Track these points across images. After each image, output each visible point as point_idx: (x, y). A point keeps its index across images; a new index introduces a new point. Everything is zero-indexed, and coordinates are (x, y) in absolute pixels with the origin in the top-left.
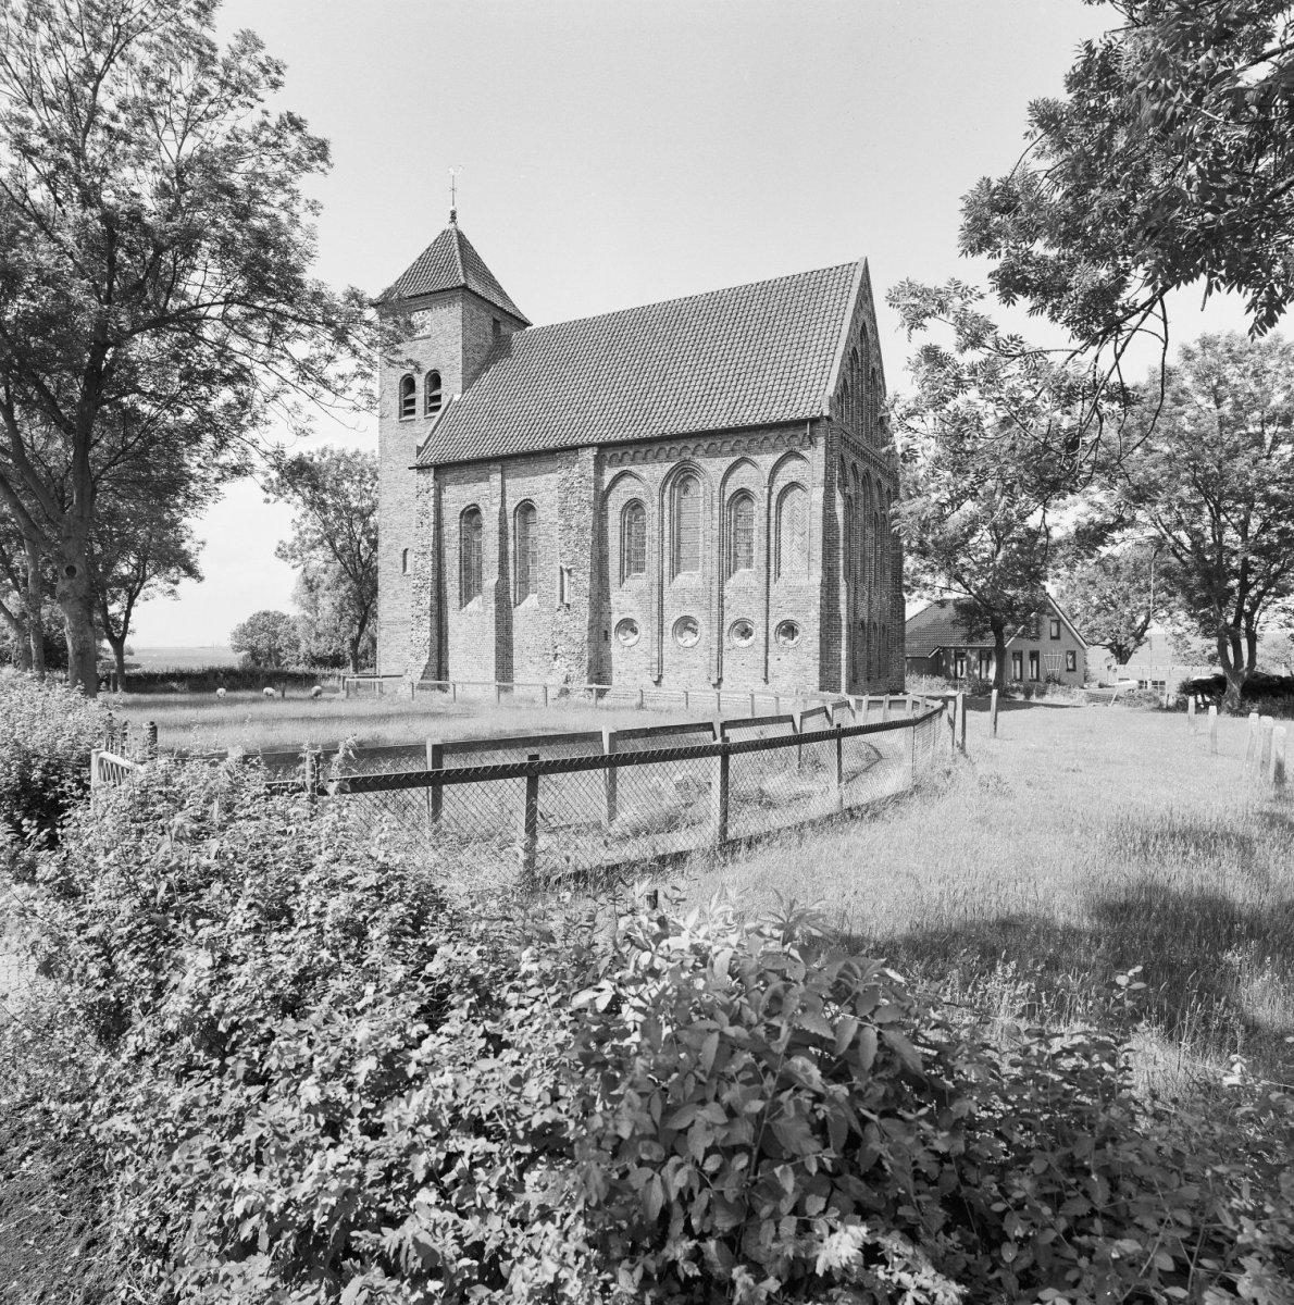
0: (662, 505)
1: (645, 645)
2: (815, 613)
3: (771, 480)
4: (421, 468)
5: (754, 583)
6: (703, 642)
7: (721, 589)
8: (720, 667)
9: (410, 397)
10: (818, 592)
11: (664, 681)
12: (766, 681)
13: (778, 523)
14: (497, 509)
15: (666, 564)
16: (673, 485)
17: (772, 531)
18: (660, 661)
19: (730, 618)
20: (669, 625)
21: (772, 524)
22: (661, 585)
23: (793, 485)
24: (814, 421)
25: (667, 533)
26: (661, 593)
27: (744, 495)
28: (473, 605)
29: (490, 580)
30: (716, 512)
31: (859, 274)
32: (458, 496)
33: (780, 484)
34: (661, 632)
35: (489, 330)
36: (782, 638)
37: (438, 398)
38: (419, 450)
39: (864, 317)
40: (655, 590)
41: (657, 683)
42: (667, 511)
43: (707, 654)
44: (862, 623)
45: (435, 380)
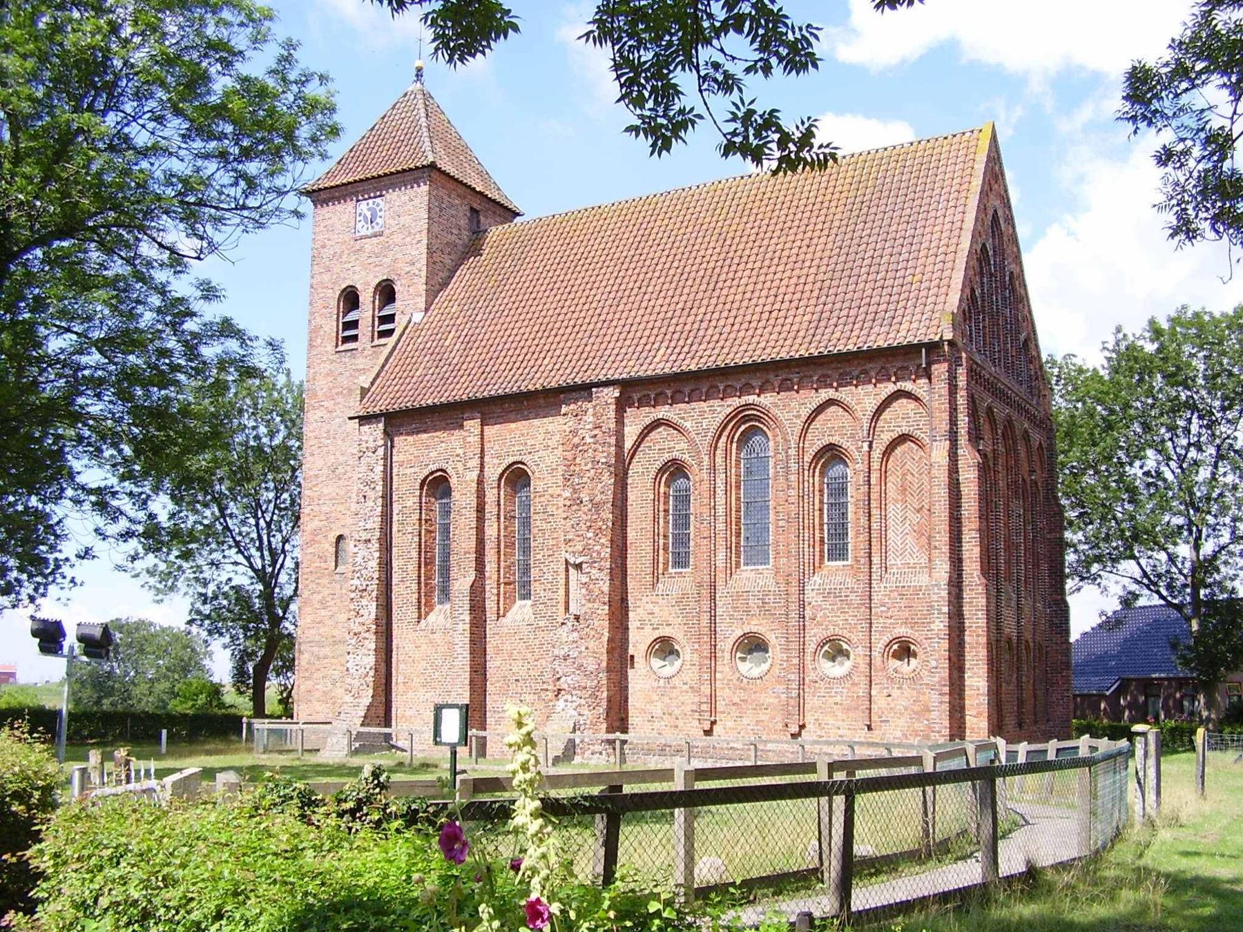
0: (713, 468)
1: (690, 675)
2: (940, 625)
3: (872, 428)
4: (364, 419)
5: (850, 583)
6: (776, 670)
7: (802, 591)
8: (801, 708)
9: (352, 316)
10: (944, 594)
12: (869, 728)
13: (883, 495)
14: (474, 475)
15: (721, 555)
16: (730, 439)
17: (874, 504)
18: (713, 698)
19: (815, 634)
20: (725, 646)
21: (874, 496)
22: (713, 586)
23: (903, 438)
24: (933, 348)
25: (721, 510)
26: (713, 599)
27: (831, 454)
28: (438, 616)
29: (462, 582)
30: (793, 478)
31: (985, 144)
32: (419, 453)
33: (886, 438)
34: (713, 656)
35: (463, 222)
37: (390, 319)
38: (364, 392)
39: (995, 202)
40: (705, 592)
41: (708, 733)
42: (721, 477)
43: (781, 688)
44: (1009, 641)
45: (387, 292)
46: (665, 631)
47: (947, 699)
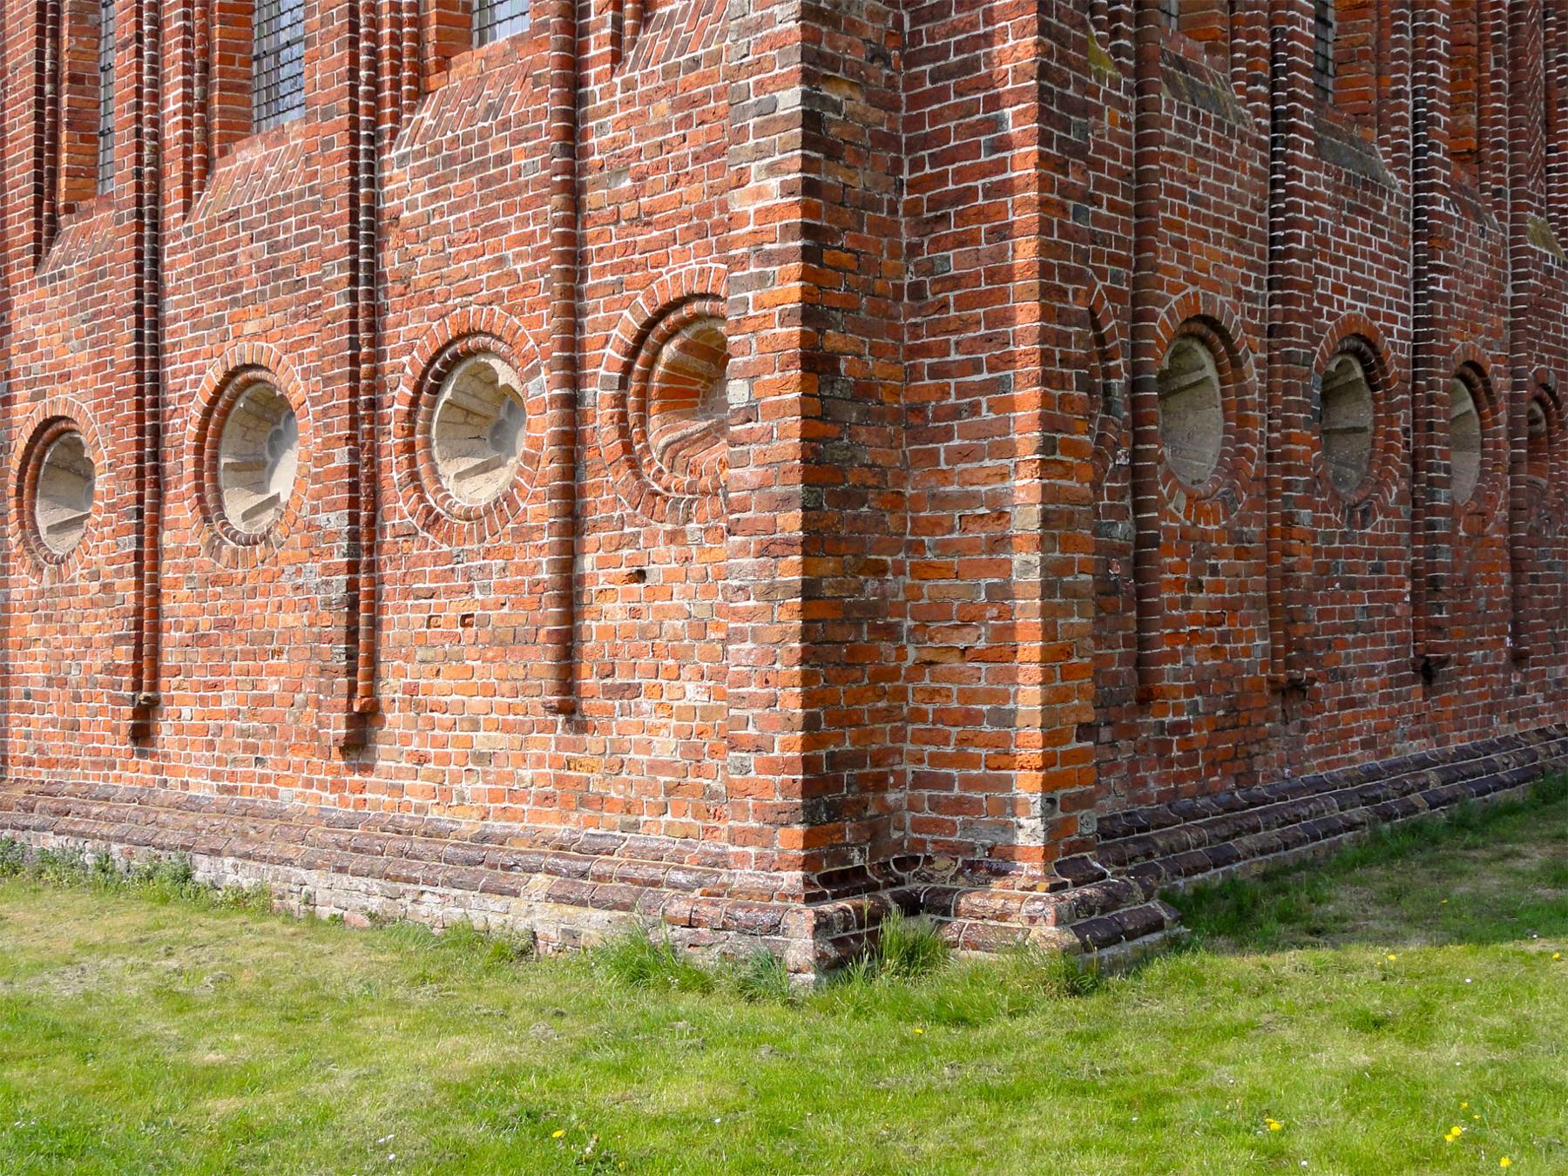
7: (365, 168)
11: (165, 729)
19: (410, 338)
36: (660, 432)
46: (61, 400)
47: (790, 570)
